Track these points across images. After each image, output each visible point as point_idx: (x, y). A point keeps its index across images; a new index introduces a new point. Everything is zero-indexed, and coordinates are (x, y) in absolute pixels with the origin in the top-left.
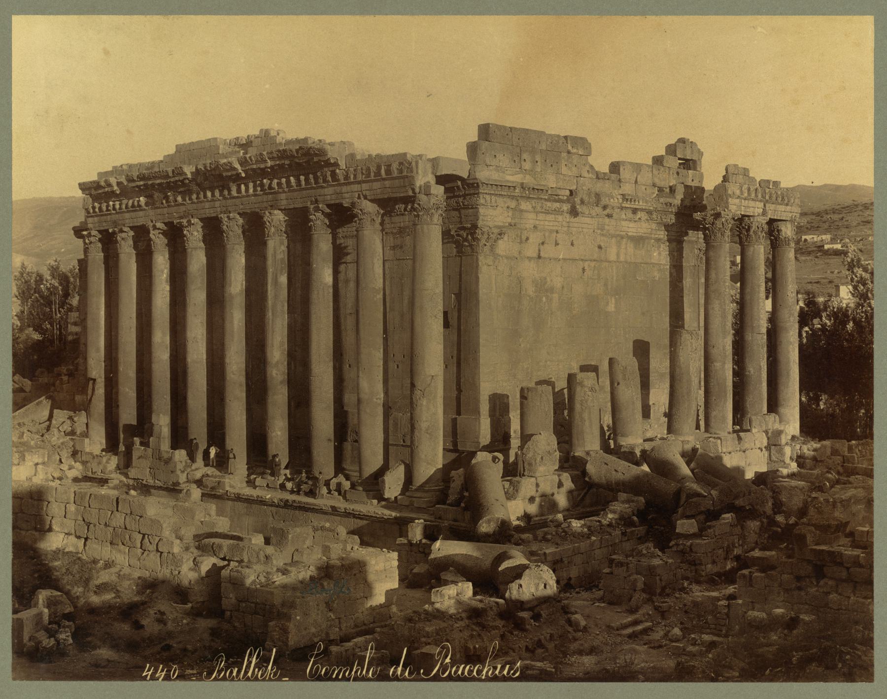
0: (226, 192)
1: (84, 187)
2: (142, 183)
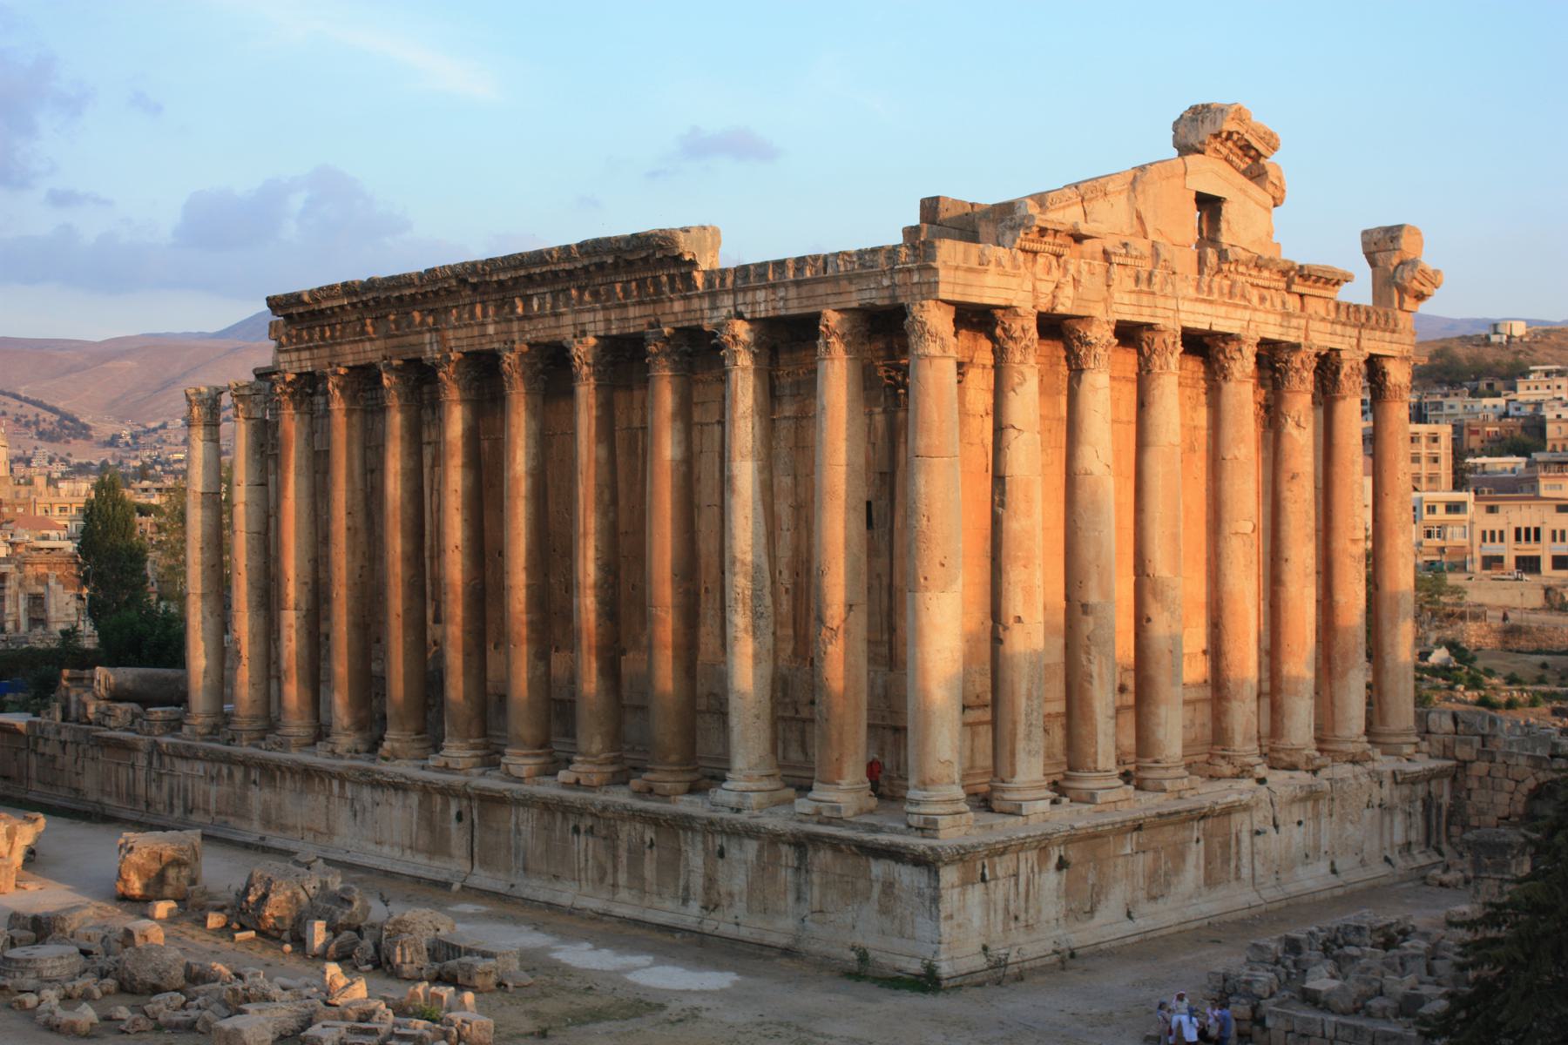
0: (507, 309)
1: (274, 303)
2: (370, 296)
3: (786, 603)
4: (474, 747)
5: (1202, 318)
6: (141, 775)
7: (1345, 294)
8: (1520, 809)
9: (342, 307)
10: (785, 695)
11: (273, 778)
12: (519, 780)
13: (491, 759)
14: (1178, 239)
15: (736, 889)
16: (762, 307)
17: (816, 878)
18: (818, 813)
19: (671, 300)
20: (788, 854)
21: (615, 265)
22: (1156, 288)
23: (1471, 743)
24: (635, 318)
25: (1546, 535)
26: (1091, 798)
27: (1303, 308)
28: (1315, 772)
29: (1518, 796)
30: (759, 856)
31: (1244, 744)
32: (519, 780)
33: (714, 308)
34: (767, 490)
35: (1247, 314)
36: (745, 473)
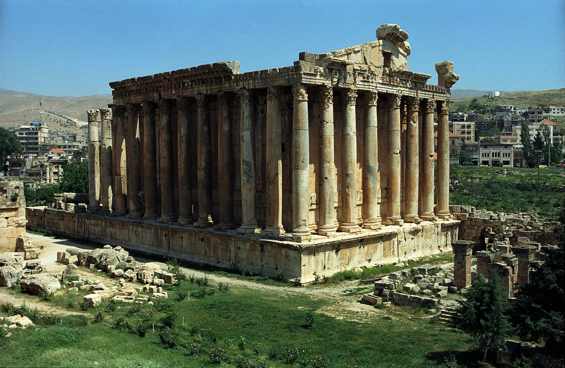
1: (112, 85)
3: (260, 175)
4: (170, 216)
5: (384, 89)
6: (76, 224)
7: (428, 82)
8: (479, 235)
9: (131, 86)
10: (260, 200)
11: (113, 225)
12: (183, 225)
13: (175, 220)
14: (377, 65)
15: (244, 258)
17: (266, 254)
18: (267, 235)
20: (259, 247)
21: (208, 73)
22: (370, 80)
23: (466, 215)
24: (215, 89)
25: (501, 155)
26: (348, 231)
27: (416, 86)
28: (418, 223)
29: (479, 231)
30: (250, 248)
31: (397, 216)
32: (183, 225)
33: (237, 85)
34: (253, 139)
35: (398, 88)
36: (246, 135)
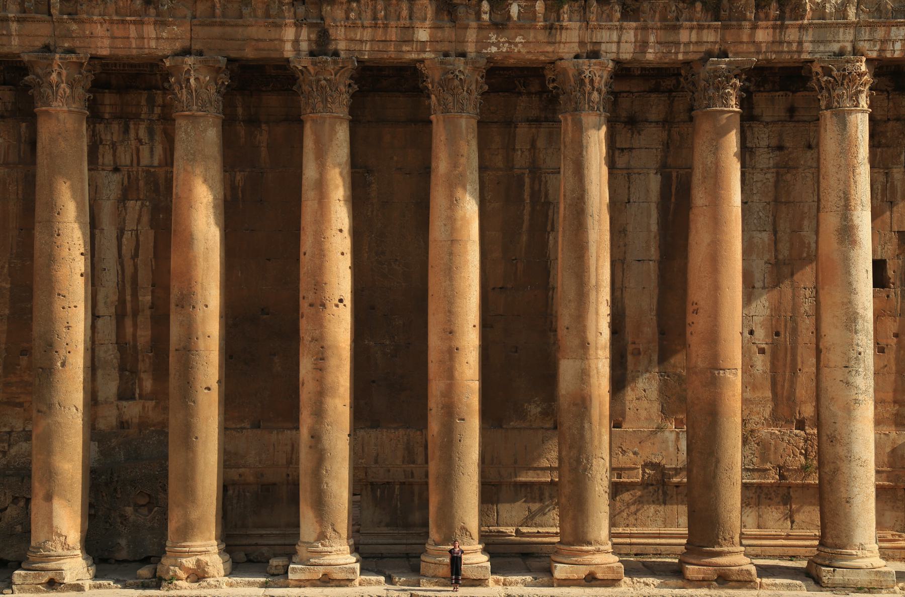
16: (898, 46)
19: (754, 27)
